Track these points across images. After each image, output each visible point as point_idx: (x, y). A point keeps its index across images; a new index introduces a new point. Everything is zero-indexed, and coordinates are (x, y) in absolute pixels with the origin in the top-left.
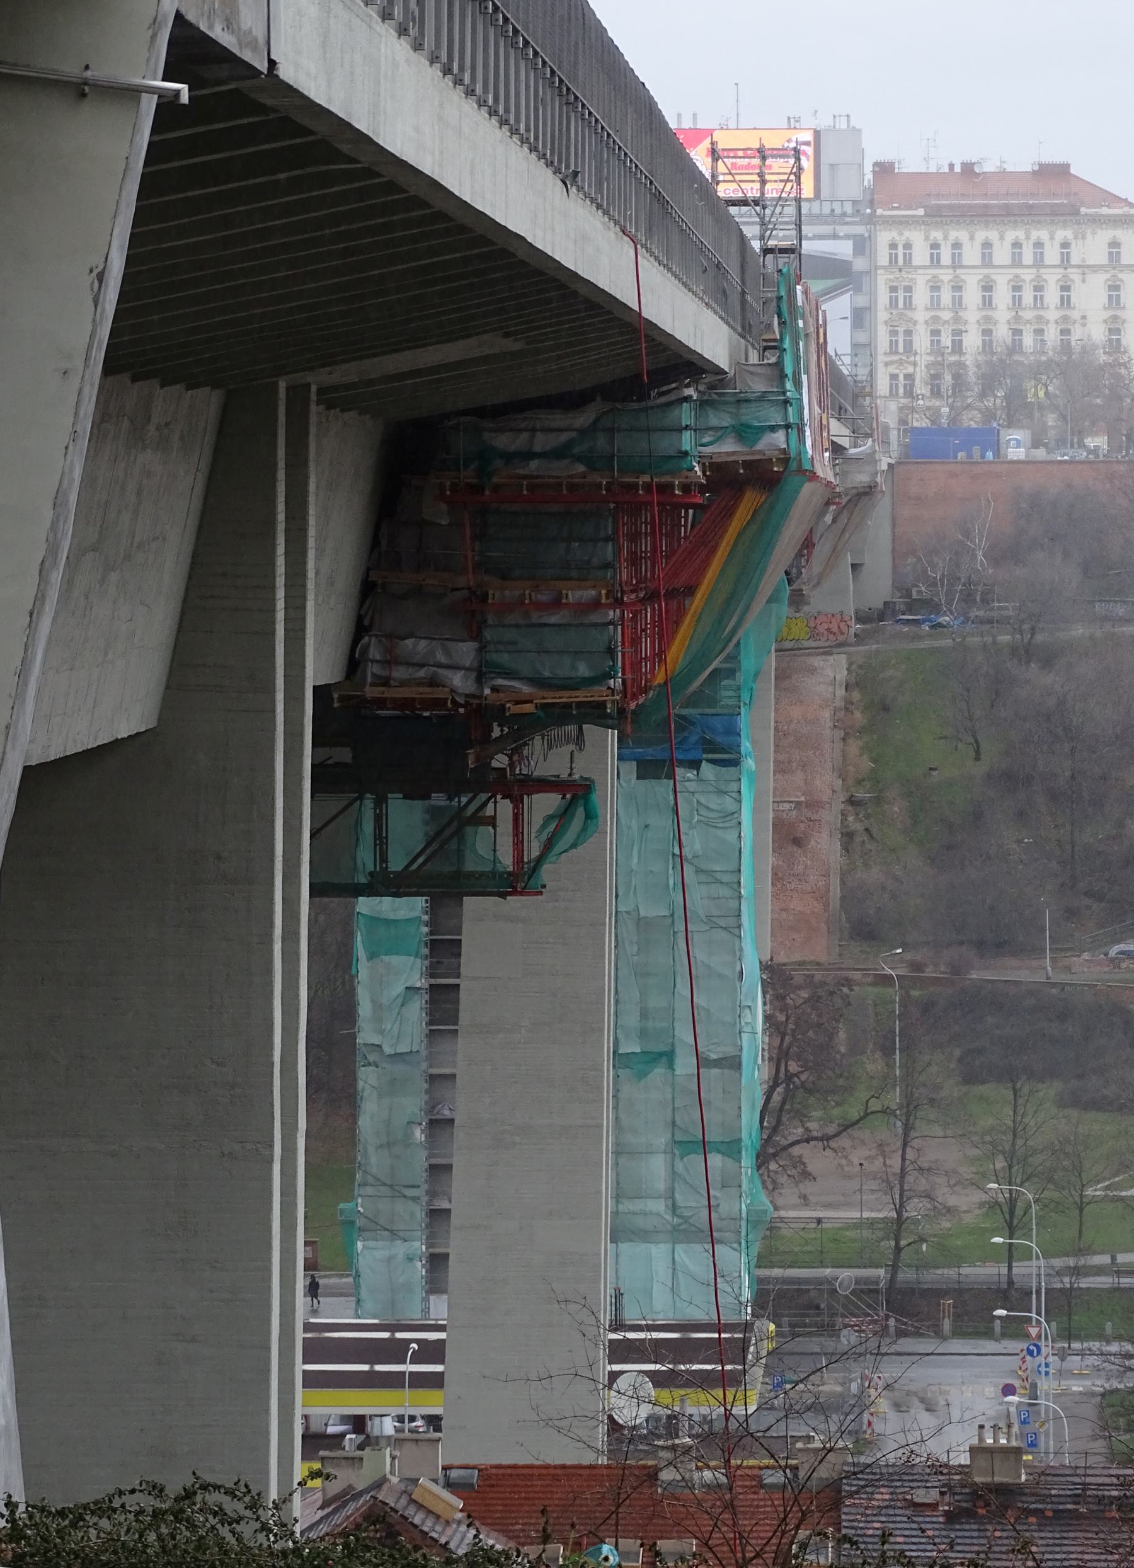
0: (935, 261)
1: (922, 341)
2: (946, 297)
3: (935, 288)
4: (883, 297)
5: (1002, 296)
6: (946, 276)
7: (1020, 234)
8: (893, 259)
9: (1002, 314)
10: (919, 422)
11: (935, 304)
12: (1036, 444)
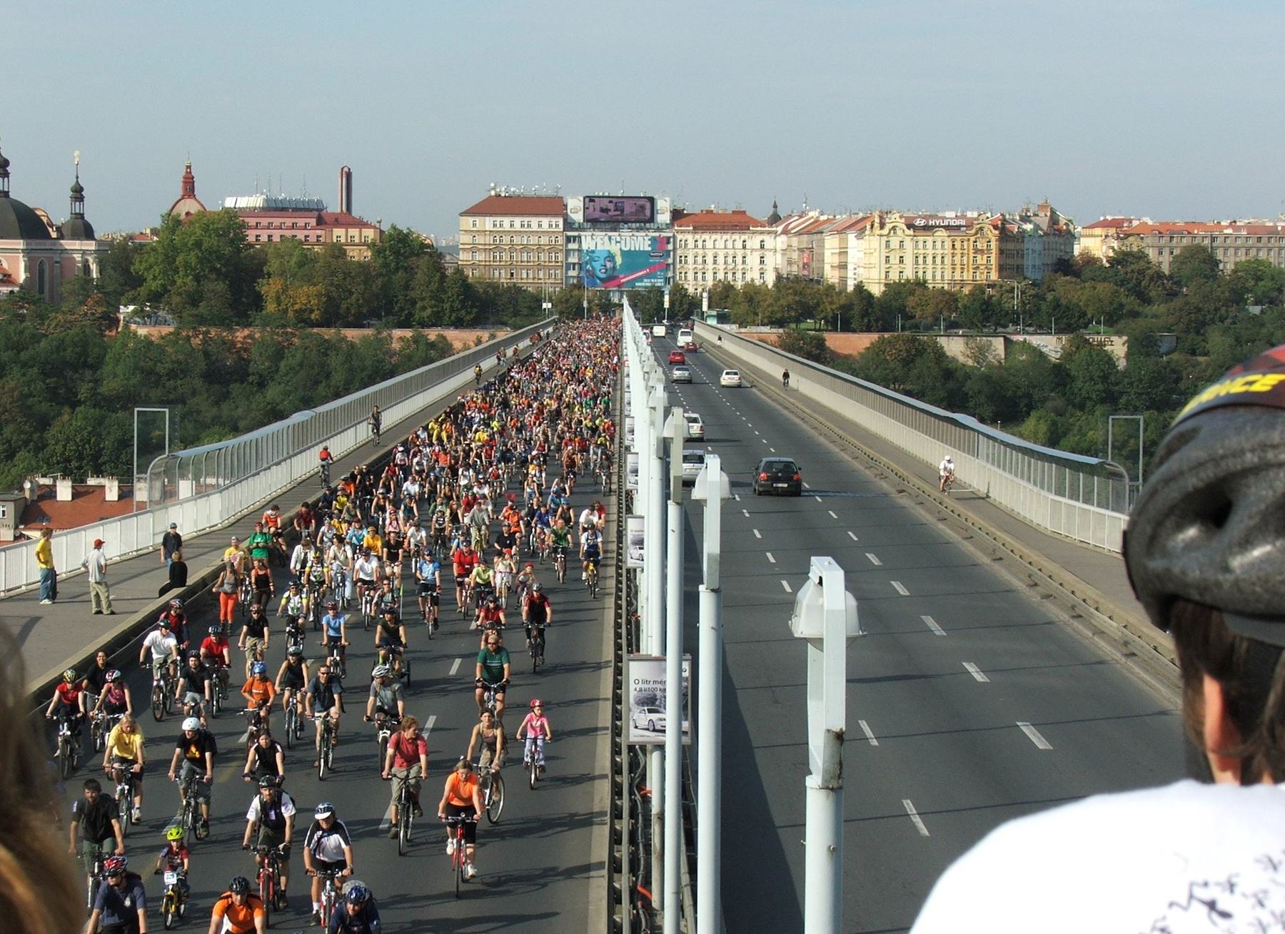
0: (696, 246)
5: (721, 260)
6: (701, 252)
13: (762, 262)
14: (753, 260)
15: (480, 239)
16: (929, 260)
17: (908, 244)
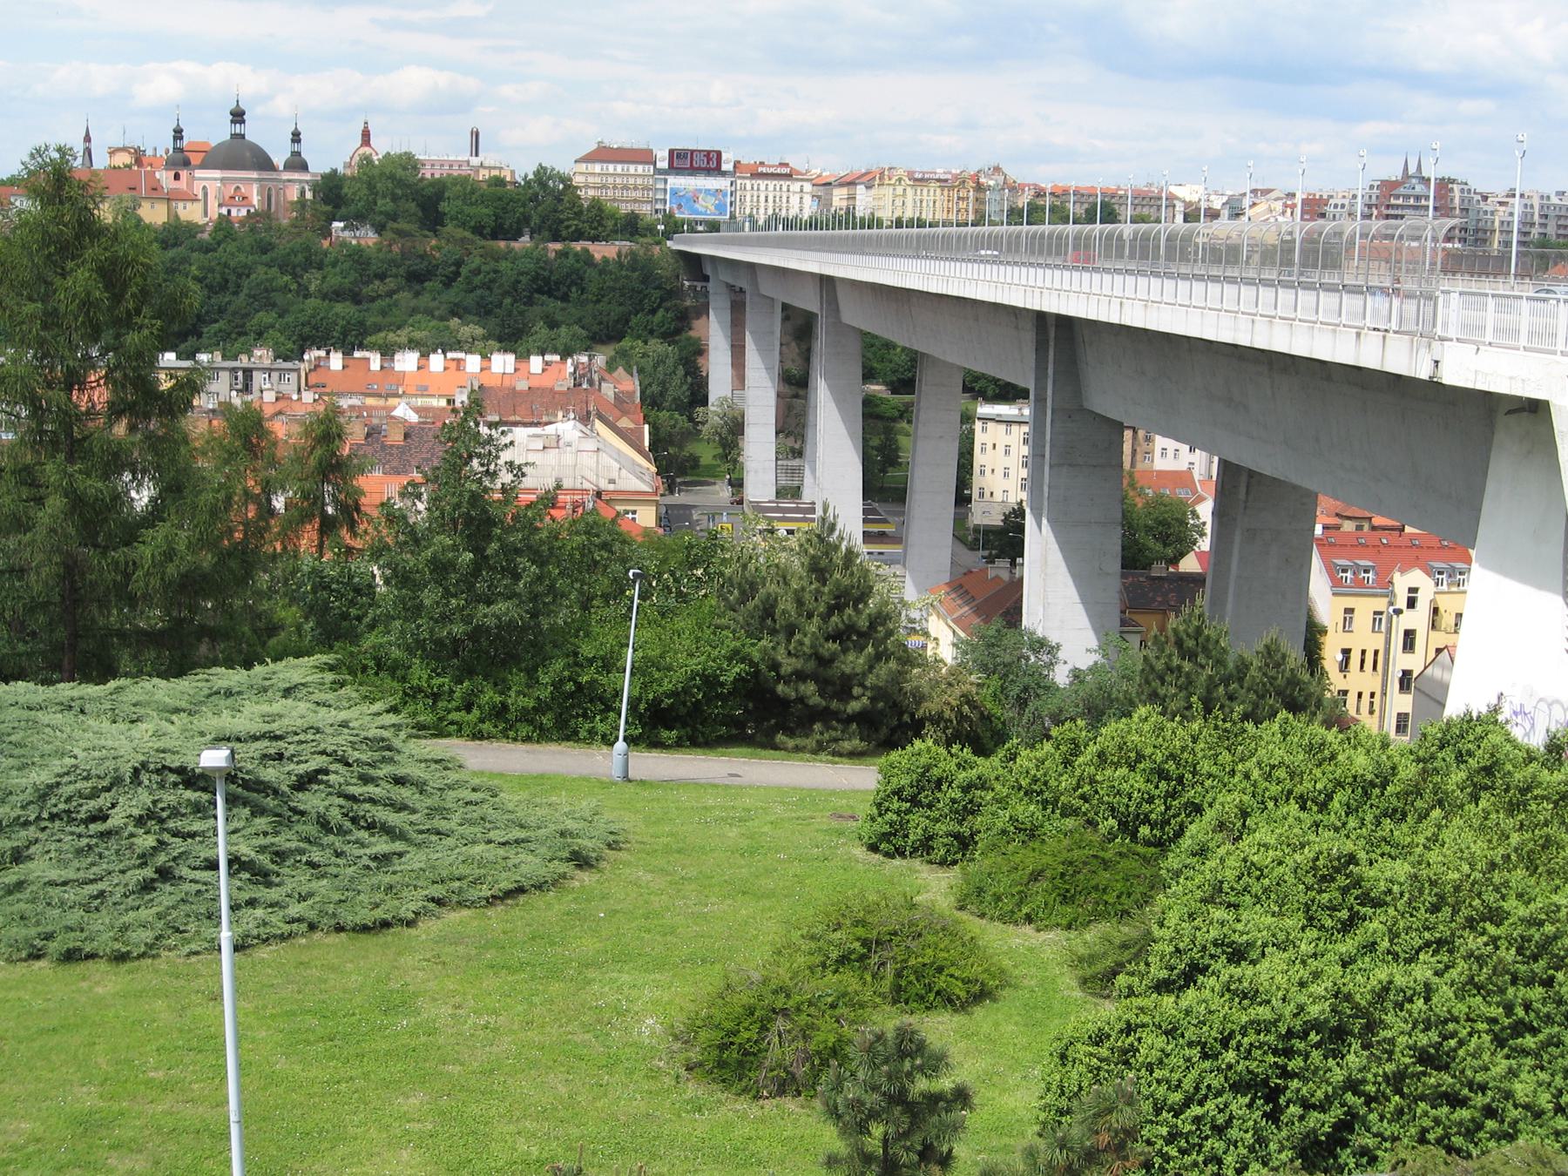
5: (771, 199)
14: (795, 200)
15: (591, 179)
16: (924, 204)
17: (910, 191)
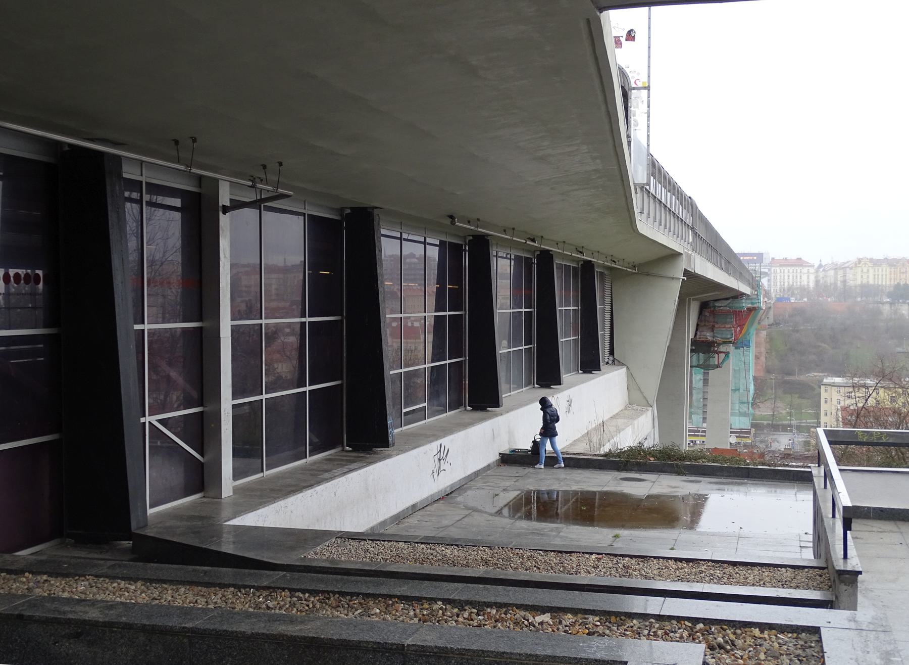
0: (781, 272)
1: (778, 284)
2: (782, 277)
3: (781, 276)
4: (772, 277)
7: (793, 268)
8: (774, 272)
9: (791, 280)
10: (778, 296)
11: (780, 279)
12: (796, 300)
13: (808, 278)
14: (805, 277)
17: (871, 271)
